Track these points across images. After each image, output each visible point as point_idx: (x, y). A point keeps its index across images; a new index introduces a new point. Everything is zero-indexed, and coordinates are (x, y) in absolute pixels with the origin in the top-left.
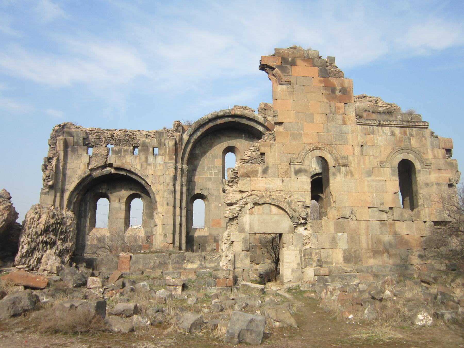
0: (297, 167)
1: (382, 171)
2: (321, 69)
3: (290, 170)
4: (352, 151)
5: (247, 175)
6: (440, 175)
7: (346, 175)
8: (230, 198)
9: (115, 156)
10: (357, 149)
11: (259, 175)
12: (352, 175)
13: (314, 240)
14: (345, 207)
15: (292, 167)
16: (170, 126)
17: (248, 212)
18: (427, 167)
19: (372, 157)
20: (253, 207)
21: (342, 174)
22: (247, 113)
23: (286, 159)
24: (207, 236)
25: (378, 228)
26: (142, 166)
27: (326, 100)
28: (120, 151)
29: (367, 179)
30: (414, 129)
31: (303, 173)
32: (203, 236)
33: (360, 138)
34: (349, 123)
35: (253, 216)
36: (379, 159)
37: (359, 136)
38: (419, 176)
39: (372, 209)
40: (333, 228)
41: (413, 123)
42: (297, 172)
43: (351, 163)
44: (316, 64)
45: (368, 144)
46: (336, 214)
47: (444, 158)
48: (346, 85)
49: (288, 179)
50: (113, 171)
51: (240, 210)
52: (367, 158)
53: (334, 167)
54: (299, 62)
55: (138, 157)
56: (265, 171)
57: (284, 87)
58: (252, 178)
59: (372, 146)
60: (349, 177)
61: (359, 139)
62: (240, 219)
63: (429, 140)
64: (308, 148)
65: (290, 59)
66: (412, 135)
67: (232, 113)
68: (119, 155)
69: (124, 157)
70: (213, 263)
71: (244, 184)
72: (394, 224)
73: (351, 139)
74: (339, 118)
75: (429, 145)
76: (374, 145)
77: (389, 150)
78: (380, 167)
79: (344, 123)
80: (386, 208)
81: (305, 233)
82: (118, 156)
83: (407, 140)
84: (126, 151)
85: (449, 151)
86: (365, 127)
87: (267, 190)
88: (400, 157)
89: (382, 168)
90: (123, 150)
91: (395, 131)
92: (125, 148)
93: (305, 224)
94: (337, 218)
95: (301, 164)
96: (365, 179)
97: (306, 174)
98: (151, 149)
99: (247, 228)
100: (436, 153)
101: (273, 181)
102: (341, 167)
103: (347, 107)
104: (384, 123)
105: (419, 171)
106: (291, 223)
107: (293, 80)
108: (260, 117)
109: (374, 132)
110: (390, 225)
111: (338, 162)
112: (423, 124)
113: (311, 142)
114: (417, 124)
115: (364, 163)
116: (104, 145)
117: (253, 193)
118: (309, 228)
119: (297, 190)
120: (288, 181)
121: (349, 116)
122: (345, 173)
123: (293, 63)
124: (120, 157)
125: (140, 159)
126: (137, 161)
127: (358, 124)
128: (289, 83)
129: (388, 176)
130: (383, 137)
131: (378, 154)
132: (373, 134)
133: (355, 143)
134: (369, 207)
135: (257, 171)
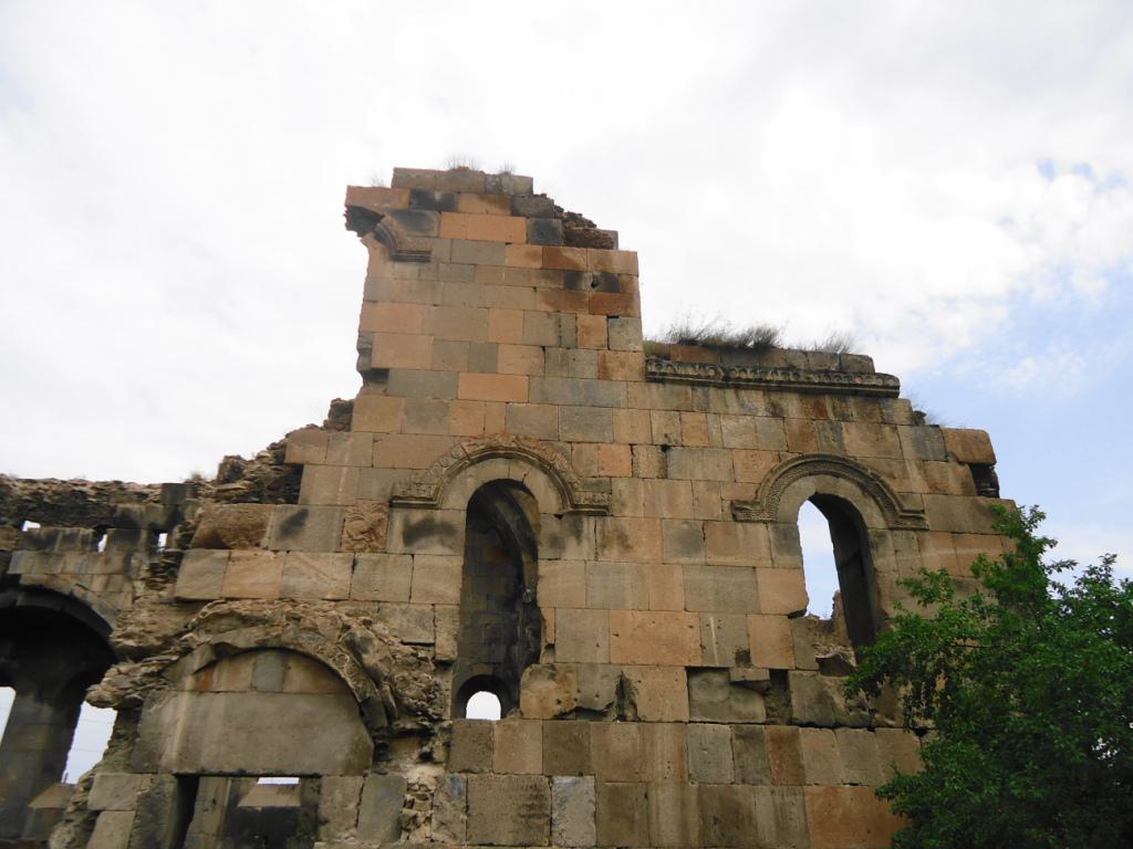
0: (417, 516)
1: (741, 536)
2: (536, 224)
3: (389, 528)
5: (215, 541)
6: (961, 551)
7: (604, 546)
8: (137, 629)
9: (33, 553)
10: (648, 459)
11: (265, 541)
13: (451, 810)
14: (592, 666)
15: (398, 519)
16: (210, 471)
17: (189, 682)
18: (909, 524)
19: (701, 486)
20: (209, 666)
21: (585, 544)
23: (376, 488)
24: (294, 809)
25: (726, 754)
26: (107, 585)
27: (544, 307)
28: (51, 539)
29: (684, 560)
30: (851, 400)
31: (435, 538)
32: (282, 809)
33: (658, 421)
34: (619, 375)
35: (205, 699)
36: (728, 494)
37: (655, 414)
38: (883, 556)
39: (704, 676)
40: (539, 754)
41: (846, 383)
42: (412, 535)
43: (623, 505)
44: (522, 210)
46: (556, 696)
47: (966, 492)
48: (617, 268)
49: (375, 557)
50: (20, 600)
51: (159, 675)
52: (683, 490)
53: (559, 517)
54: (466, 202)
55: (103, 558)
56: (292, 527)
57: (409, 269)
58: (236, 553)
60: (613, 553)
61: (655, 425)
62: (149, 713)
63: (904, 431)
65: (438, 196)
66: (845, 418)
68: (47, 550)
69: (60, 556)
71: (201, 574)
72: (795, 736)
73: (626, 426)
75: (908, 449)
76: (709, 447)
77: (766, 463)
78: (731, 519)
79: (604, 373)
80: (757, 672)
81: (420, 774)
82: (46, 554)
83: (830, 434)
84: (69, 539)
85: (982, 474)
86: (677, 388)
87: (287, 598)
89: (739, 526)
90: (60, 537)
91: (784, 404)
92: (68, 530)
93: (425, 735)
94: (558, 708)
95: (429, 504)
96: (675, 561)
97: (449, 541)
98: (144, 535)
99: (171, 751)
100: (937, 476)
101: (317, 564)
102: (585, 519)
103: (617, 329)
104: (744, 376)
105: (881, 536)
106: (364, 732)
107: (439, 249)
109: (708, 404)
110: (779, 741)
111: (571, 500)
112: (880, 382)
113: (479, 431)
114: (858, 381)
115: (672, 504)
116: (11, 522)
117: (234, 605)
118: (439, 755)
119: (406, 599)
120: (377, 563)
121: (621, 355)
122: (599, 537)
123: (448, 205)
124: (47, 555)
125: (107, 561)
126: (98, 568)
127: (652, 378)
128: (422, 257)
129: (764, 551)
130: (743, 421)
131: (722, 477)
132: (705, 410)
133: (641, 438)
134: (692, 671)
135: (259, 528)
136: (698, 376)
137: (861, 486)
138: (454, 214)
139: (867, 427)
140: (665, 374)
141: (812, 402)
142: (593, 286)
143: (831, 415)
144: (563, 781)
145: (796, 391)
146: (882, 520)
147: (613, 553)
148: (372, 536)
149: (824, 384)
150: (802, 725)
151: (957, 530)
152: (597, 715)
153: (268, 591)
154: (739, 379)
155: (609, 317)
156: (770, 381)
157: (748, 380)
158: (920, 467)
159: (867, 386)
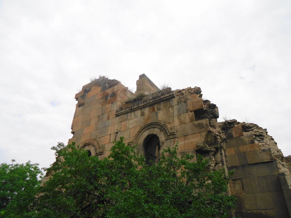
4: (109, 140)
6: (186, 142)
18: (171, 137)
45: (122, 130)
47: (191, 120)
59: (124, 131)
66: (159, 109)
74: (106, 115)
75: (176, 113)
77: (138, 129)
79: (108, 119)
83: (155, 116)
86: (122, 116)
88: (146, 134)
100: (183, 118)
103: (113, 106)
104: (135, 107)
112: (168, 95)
114: (162, 97)
123: (89, 90)
130: (134, 120)
136: (125, 111)
137: (160, 129)
138: (90, 92)
139: (165, 110)
140: (118, 114)
141: (152, 107)
142: (110, 97)
143: (156, 110)
145: (148, 106)
146: (164, 138)
149: (153, 102)
151: (186, 135)
154: (134, 109)
155: (112, 103)
156: (140, 106)
157: (136, 108)
158: (178, 117)
159: (165, 98)
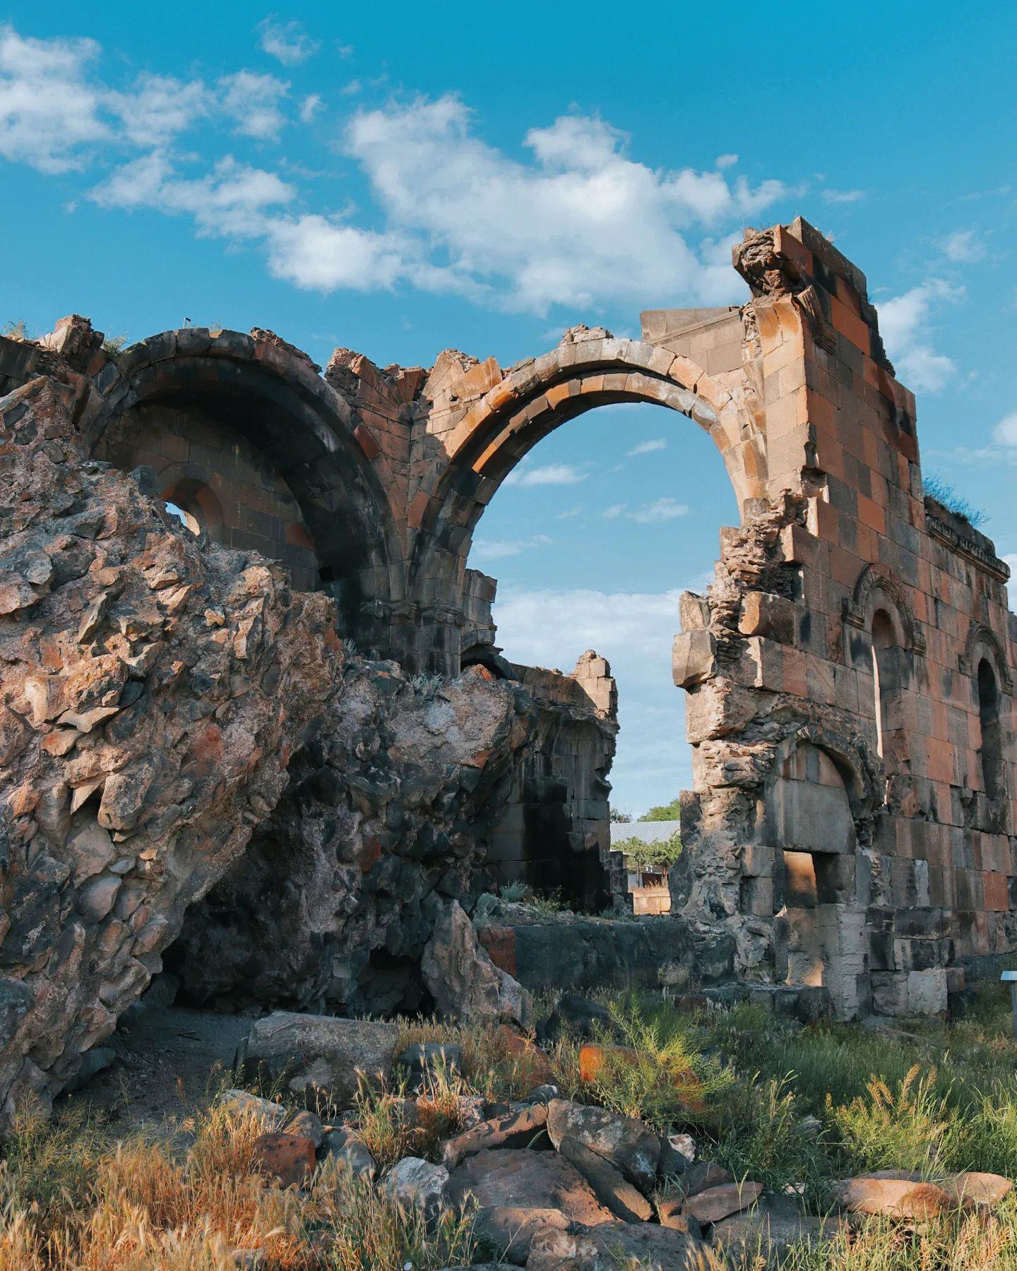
12: (928, 685)
22: (302, 365)
29: (945, 700)
54: (840, 288)
60: (924, 688)
64: (872, 576)
67: (259, 356)
70: (719, 961)
88: (980, 651)
108: (339, 397)
134: (952, 786)
144: (919, 862)
147: (924, 688)
148: (838, 644)
150: (982, 831)
152: (922, 813)
153: (801, 691)
